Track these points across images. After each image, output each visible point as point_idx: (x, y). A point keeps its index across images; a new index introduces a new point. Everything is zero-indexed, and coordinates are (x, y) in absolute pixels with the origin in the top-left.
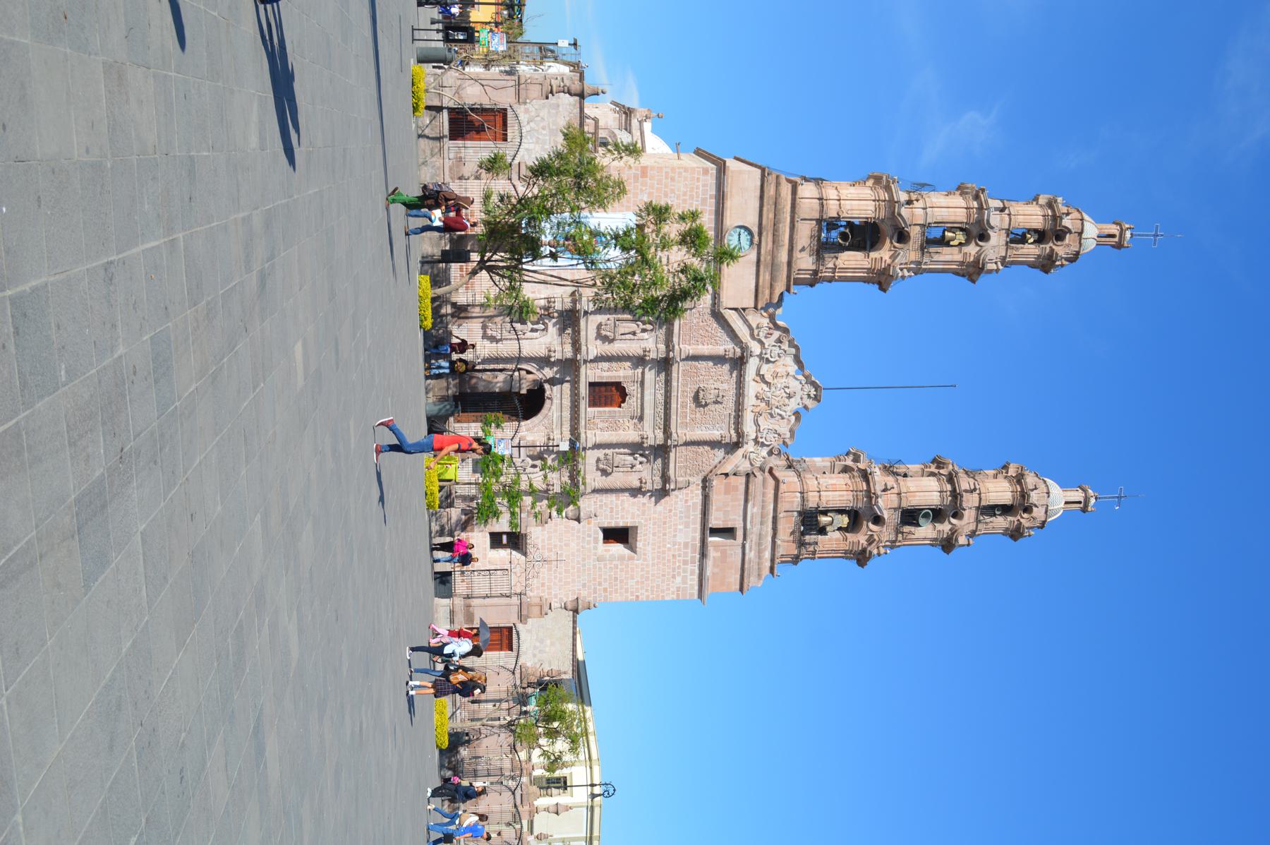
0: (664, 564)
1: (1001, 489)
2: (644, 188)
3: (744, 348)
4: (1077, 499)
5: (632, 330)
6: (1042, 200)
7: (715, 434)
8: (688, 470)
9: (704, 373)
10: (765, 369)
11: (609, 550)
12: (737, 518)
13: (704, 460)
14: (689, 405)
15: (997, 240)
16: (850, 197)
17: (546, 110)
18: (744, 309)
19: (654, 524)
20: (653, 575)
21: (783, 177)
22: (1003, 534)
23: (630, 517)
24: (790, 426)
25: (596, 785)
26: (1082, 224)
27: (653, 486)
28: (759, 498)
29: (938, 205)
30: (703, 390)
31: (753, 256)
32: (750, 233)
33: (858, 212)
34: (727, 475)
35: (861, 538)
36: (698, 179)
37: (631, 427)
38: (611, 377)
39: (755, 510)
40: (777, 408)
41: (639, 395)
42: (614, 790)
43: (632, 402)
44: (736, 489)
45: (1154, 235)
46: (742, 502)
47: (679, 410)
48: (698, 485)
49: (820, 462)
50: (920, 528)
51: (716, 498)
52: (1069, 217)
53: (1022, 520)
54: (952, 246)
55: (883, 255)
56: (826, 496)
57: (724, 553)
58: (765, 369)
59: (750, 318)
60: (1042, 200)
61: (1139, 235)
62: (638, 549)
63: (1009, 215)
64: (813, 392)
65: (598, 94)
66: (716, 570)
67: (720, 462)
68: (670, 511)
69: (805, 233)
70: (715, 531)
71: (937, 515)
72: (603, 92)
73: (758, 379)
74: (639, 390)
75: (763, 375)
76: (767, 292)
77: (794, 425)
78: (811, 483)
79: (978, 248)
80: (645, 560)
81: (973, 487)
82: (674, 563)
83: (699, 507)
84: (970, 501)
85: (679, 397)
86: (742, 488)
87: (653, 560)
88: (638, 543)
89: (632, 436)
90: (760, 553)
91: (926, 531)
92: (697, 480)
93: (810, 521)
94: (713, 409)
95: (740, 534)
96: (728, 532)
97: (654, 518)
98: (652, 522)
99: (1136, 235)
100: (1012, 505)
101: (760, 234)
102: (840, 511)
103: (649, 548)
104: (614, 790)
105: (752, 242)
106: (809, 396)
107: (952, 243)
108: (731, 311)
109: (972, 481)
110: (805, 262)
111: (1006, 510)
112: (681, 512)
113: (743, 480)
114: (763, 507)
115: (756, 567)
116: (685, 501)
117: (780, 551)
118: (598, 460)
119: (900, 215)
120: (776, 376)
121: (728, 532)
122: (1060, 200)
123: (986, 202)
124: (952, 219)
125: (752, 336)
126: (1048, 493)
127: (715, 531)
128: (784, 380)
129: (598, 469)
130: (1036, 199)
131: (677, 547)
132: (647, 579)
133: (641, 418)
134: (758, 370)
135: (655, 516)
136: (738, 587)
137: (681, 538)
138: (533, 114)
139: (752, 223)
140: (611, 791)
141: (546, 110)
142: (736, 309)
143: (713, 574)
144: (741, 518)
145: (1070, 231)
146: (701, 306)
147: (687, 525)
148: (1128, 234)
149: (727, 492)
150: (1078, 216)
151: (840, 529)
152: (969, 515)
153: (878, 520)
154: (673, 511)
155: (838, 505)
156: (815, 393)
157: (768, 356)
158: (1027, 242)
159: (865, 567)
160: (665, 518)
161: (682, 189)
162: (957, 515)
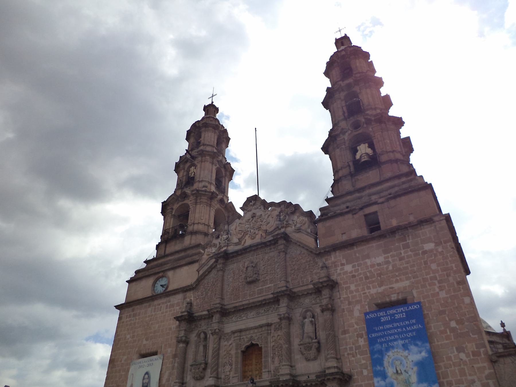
2: (120, 359)
13: (304, 261)
14: (260, 288)
19: (369, 288)
24: (277, 208)
27: (325, 298)
30: (246, 279)
31: (170, 274)
37: (279, 333)
40: (262, 222)
41: (252, 332)
43: (256, 338)
47: (264, 294)
48: (326, 260)
58: (235, 240)
62: (400, 297)
64: (253, 202)
67: (303, 247)
68: (354, 276)
74: (247, 332)
82: (408, 257)
83: (348, 252)
85: (254, 297)
87: (408, 279)
88: (393, 299)
92: (320, 262)
94: (263, 267)
97: (363, 289)
98: (367, 291)
105: (162, 277)
106: (254, 204)
112: (353, 267)
118: (308, 360)
129: (315, 359)
131: (390, 260)
132: (435, 278)
133: (269, 325)
135: (360, 290)
137: (380, 259)
139: (150, 281)
146: (192, 299)
147: (368, 257)
154: (354, 274)
156: (252, 201)
160: (361, 279)
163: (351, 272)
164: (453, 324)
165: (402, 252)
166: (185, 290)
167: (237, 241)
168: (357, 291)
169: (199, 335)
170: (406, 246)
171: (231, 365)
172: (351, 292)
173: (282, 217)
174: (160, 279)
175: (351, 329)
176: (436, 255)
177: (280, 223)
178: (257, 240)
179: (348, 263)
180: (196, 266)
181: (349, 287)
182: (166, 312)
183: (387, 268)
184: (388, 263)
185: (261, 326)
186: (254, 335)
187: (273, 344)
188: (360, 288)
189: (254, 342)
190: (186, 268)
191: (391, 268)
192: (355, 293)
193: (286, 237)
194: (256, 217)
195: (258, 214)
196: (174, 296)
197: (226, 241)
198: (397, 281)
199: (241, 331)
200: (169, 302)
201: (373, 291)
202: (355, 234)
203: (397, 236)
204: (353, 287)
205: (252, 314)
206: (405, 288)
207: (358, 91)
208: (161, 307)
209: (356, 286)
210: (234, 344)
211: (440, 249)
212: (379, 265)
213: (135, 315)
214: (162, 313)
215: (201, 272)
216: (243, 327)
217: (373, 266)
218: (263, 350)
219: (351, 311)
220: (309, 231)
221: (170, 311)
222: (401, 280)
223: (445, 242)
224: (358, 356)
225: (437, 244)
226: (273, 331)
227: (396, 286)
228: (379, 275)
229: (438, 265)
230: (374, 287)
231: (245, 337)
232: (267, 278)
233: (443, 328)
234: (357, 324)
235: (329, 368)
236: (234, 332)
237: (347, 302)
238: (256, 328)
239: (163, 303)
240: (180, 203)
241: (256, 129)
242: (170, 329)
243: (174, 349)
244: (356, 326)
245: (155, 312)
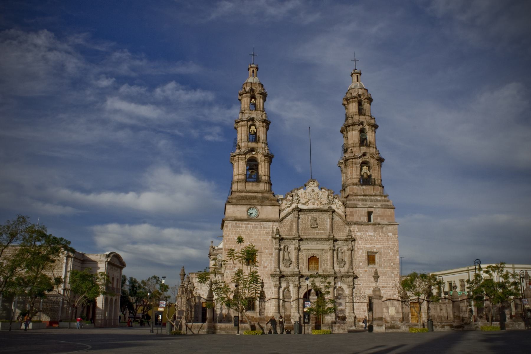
0: (383, 240)
1: (352, 107)
3: (294, 210)
4: (356, 77)
5: (287, 254)
6: (240, 98)
7: (329, 220)
8: (344, 231)
9: (305, 226)
10: (303, 201)
11: (378, 263)
12: (364, 211)
13: (340, 225)
15: (254, 115)
16: (237, 171)
17: (203, 287)
18: (280, 210)
19: (366, 244)
20: (388, 245)
21: (230, 197)
22: (370, 104)
23: (363, 255)
24: (326, 191)
25: (475, 267)
26: (249, 83)
28: (355, 202)
29: (241, 137)
31: (259, 207)
32: (250, 208)
33: (243, 168)
34: (346, 216)
35: (373, 162)
36: (230, 229)
37: (327, 254)
38: (306, 263)
39: (360, 204)
41: (314, 251)
42: (477, 259)
43: (317, 254)
44: (351, 212)
45: (253, 56)
46: (357, 209)
49: (343, 179)
50: (368, 138)
51: (355, 219)
52: (246, 88)
53: (364, 98)
54: (256, 131)
55: (260, 157)
56: (355, 176)
57: (379, 216)
59: (283, 208)
60: (240, 98)
61: (253, 61)
62: (377, 251)
63: (244, 110)
64: (312, 183)
65: (184, 269)
66: (385, 219)
68: (361, 238)
69: (250, 187)
70: (369, 220)
71: (362, 131)
72: (183, 267)
73: (307, 204)
74: (311, 251)
75: (305, 202)
76: (273, 202)
77: (325, 190)
78: (350, 181)
79: (257, 121)
80: (381, 248)
81: (351, 118)
82: (382, 236)
83: (359, 226)
84: (357, 118)
86: (351, 209)
87: (381, 245)
88: (374, 251)
89: (329, 254)
90: (378, 201)
91: (370, 136)
93: (366, 181)
95: (370, 210)
96: (370, 214)
99: (253, 62)
100: (358, 102)
101: (250, 205)
102: (361, 169)
103: (376, 246)
104: (477, 259)
107: (255, 131)
108: (280, 216)
109: (349, 119)
110: (262, 187)
111: (360, 104)
112: (361, 234)
113: (347, 208)
114: (359, 200)
115: (384, 203)
116: (358, 232)
117: (378, 193)
119: (244, 152)
120: (305, 197)
121: (370, 214)
122: (239, 92)
123: (239, 119)
124: (246, 132)
125: (289, 207)
126: (353, 89)
127: (369, 220)
128: (307, 194)
130: (240, 100)
131: (376, 235)
133: (323, 250)
134: (303, 204)
136: (392, 210)
137: (372, 234)
138: (204, 292)
140: (478, 261)
141: (203, 287)
143: (387, 220)
144: (364, 209)
145: (251, 88)
147: (367, 231)
148: (253, 66)
149: (353, 216)
150: (245, 84)
151: (369, 169)
152: (362, 118)
153: (364, 155)
155: (359, 171)
157: (297, 200)
158: (255, 103)
159: (384, 159)
161: (233, 235)
162: (362, 123)
163: (360, 236)
164: (392, 264)
165: (381, 233)
167: (304, 203)
168: (361, 244)
169: (284, 247)
170: (382, 232)
171: (303, 263)
172: (359, 244)
173: (330, 199)
174: (252, 209)
175: (358, 259)
176: (392, 239)
177: (329, 201)
178: (315, 206)
179: (360, 231)
180: (277, 209)
181: (358, 242)
182: (262, 230)
183: (374, 238)
184: (374, 236)
185: (319, 250)
186: (315, 253)
187: (324, 258)
188: (363, 244)
189: (315, 256)
190: (270, 207)
191: (375, 239)
192: (360, 245)
193: (334, 211)
194: (315, 193)
195: (315, 191)
196: (265, 222)
197: (297, 200)
198: (377, 245)
199: (309, 250)
200: (263, 225)
201: (368, 246)
203: (380, 226)
204: (360, 242)
205: (314, 243)
206: (379, 248)
207: (367, 130)
208: (257, 227)
209: (361, 242)
210: (304, 255)
211: (393, 237)
212: (371, 236)
213: (237, 227)
214: (258, 230)
215: (283, 214)
216: (309, 248)
217: (369, 236)
218: (319, 260)
219: (358, 252)
220: (343, 210)
221: (264, 230)
222: (378, 245)
223: (396, 234)
224: (359, 269)
225: (393, 234)
226: (324, 253)
227: (376, 246)
228: (371, 240)
229: (392, 242)
230: (368, 245)
231: (310, 253)
232: (321, 228)
233: (389, 265)
234: (360, 257)
235: (350, 272)
236: (304, 250)
237: (357, 248)
238: (316, 250)
239: (258, 225)
240: (251, 155)
241: (310, 128)
242: (266, 240)
243: (270, 251)
244: (359, 258)
245: (253, 228)
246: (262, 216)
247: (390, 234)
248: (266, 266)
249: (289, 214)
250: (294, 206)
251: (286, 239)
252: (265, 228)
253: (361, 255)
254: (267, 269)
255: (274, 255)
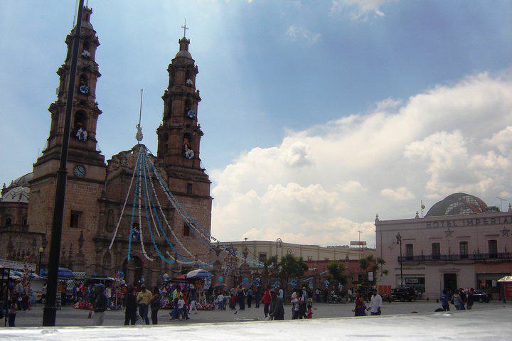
31: (86, 166)
86: (174, 180)
134: (130, 168)
137: (190, 206)
142: (107, 175)
147: (185, 203)
166: (101, 183)
190: (97, 168)
202: (183, 190)
246: (89, 176)
247: (205, 208)
248: (89, 229)
249: (115, 177)
250: (121, 168)
251: (111, 203)
252: (91, 189)
253: (179, 225)
254: (89, 233)
255: (98, 218)
